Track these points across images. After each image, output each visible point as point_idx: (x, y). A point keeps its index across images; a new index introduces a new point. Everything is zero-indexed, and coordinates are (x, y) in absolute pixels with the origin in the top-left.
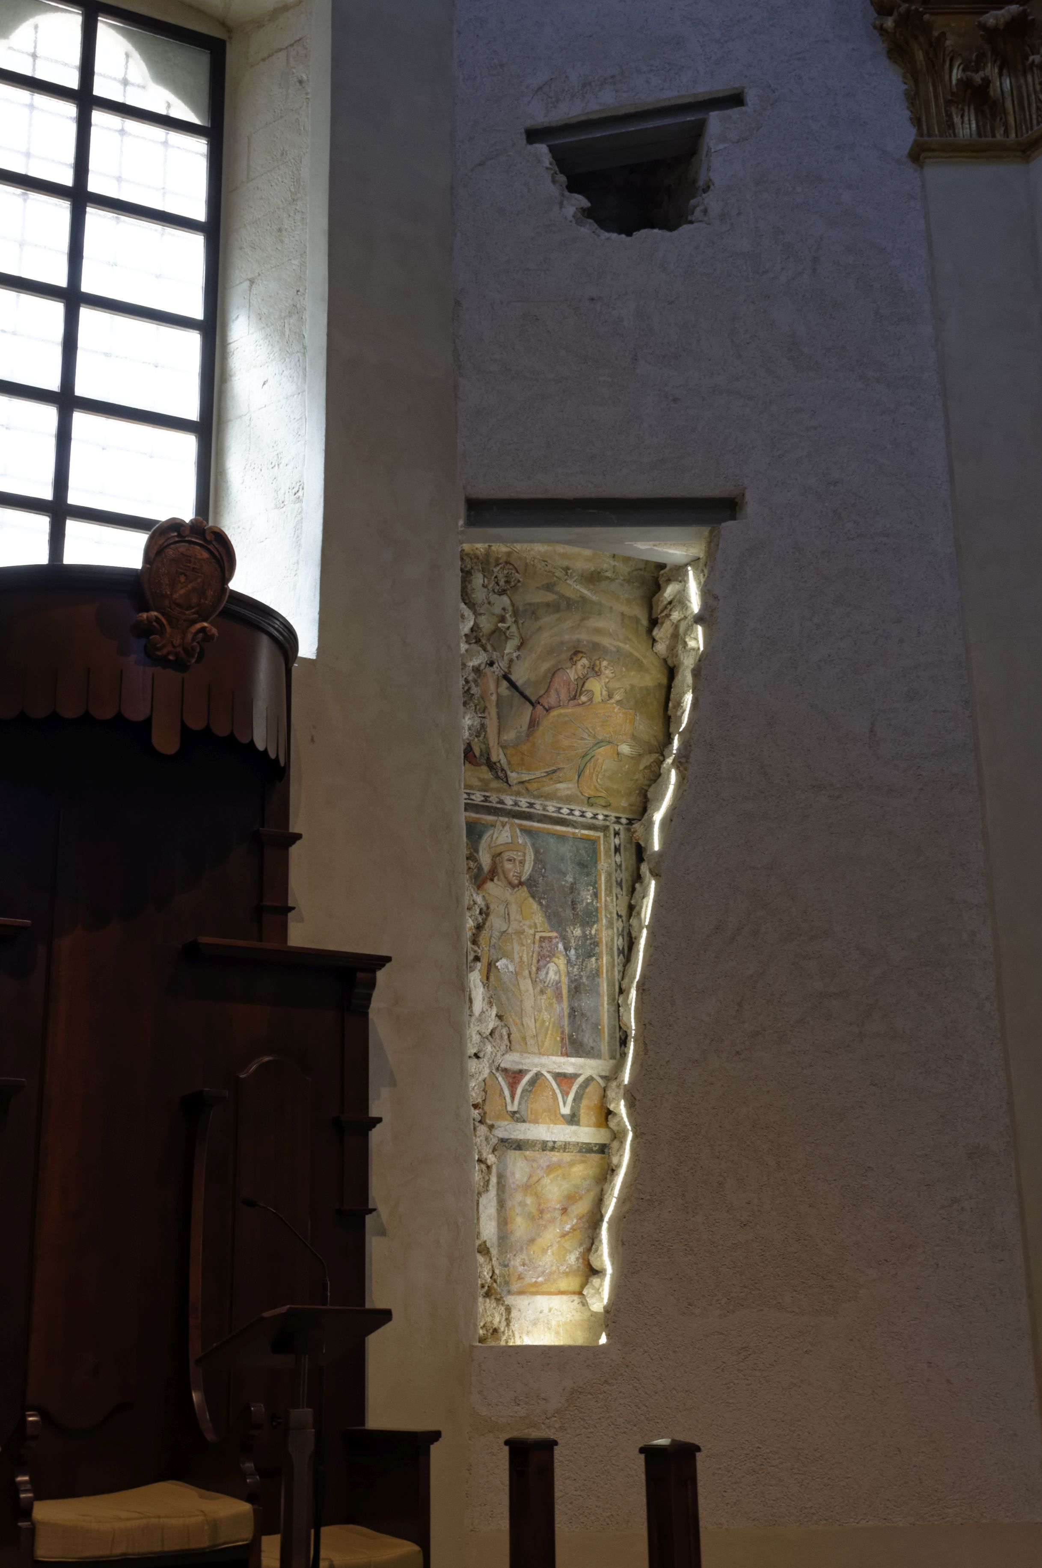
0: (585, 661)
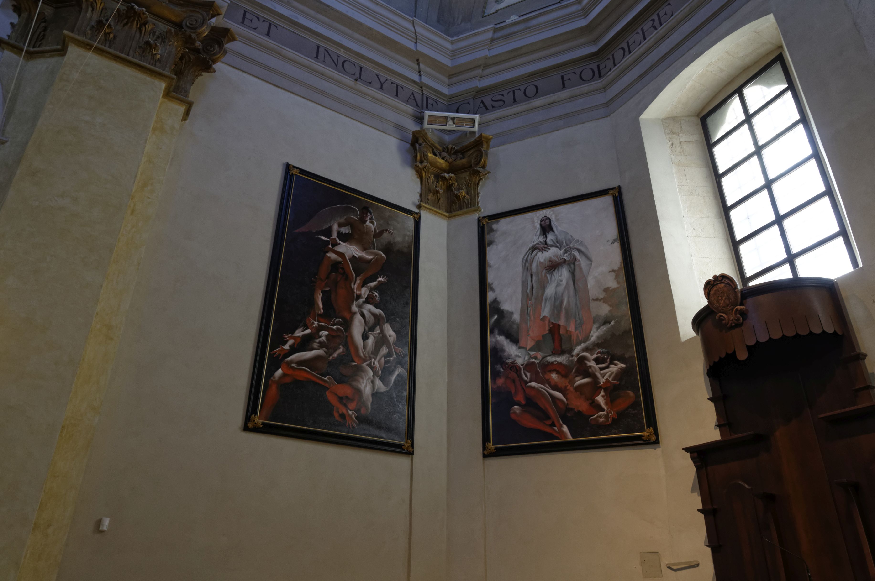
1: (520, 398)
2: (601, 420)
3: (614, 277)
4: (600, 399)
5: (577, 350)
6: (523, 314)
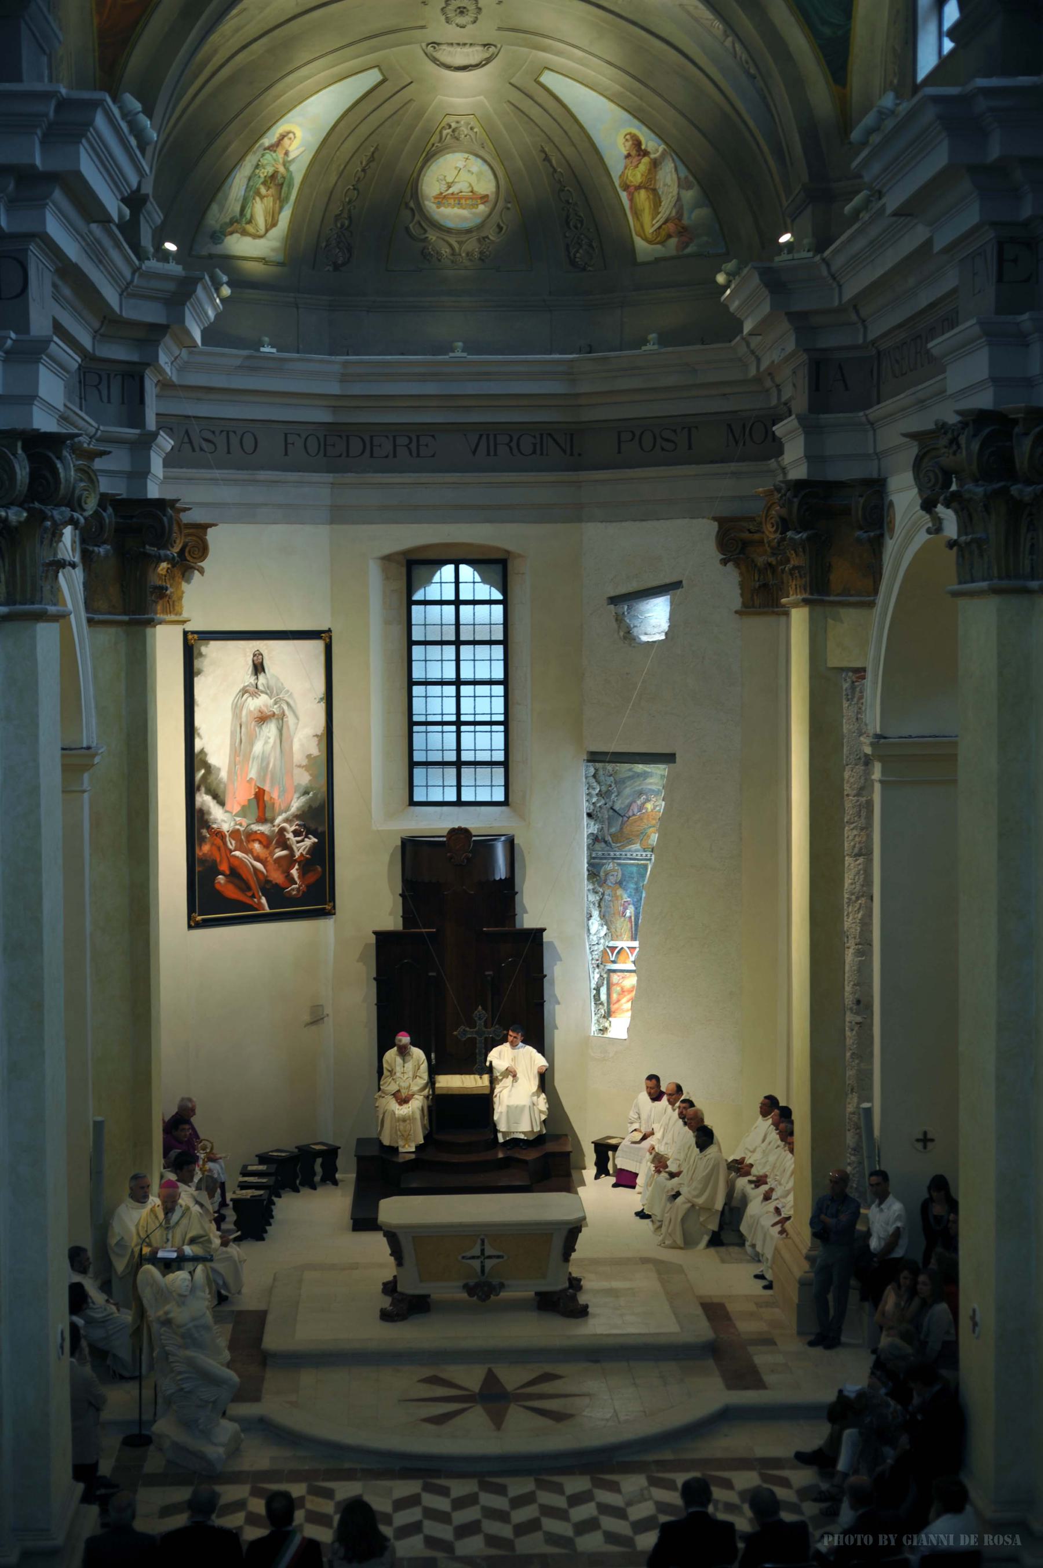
0: (644, 797)
1: (224, 867)
2: (294, 893)
3: (317, 743)
4: (294, 872)
5: (279, 820)
6: (230, 773)
